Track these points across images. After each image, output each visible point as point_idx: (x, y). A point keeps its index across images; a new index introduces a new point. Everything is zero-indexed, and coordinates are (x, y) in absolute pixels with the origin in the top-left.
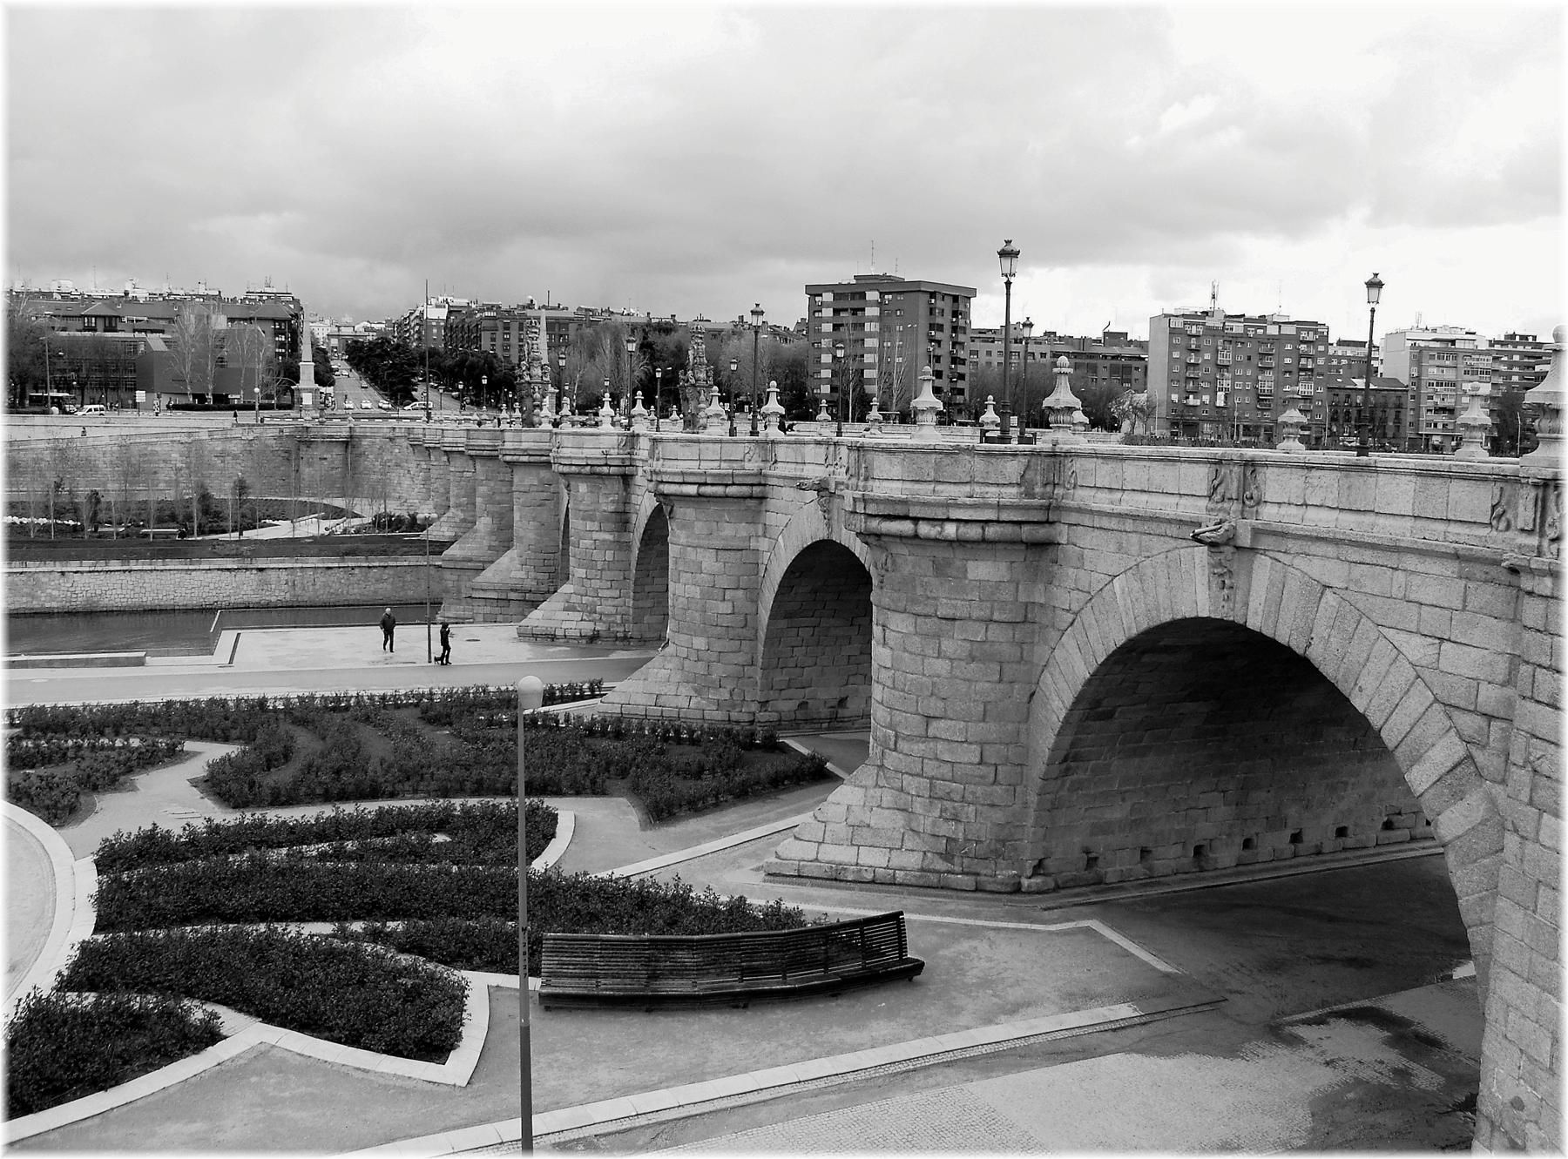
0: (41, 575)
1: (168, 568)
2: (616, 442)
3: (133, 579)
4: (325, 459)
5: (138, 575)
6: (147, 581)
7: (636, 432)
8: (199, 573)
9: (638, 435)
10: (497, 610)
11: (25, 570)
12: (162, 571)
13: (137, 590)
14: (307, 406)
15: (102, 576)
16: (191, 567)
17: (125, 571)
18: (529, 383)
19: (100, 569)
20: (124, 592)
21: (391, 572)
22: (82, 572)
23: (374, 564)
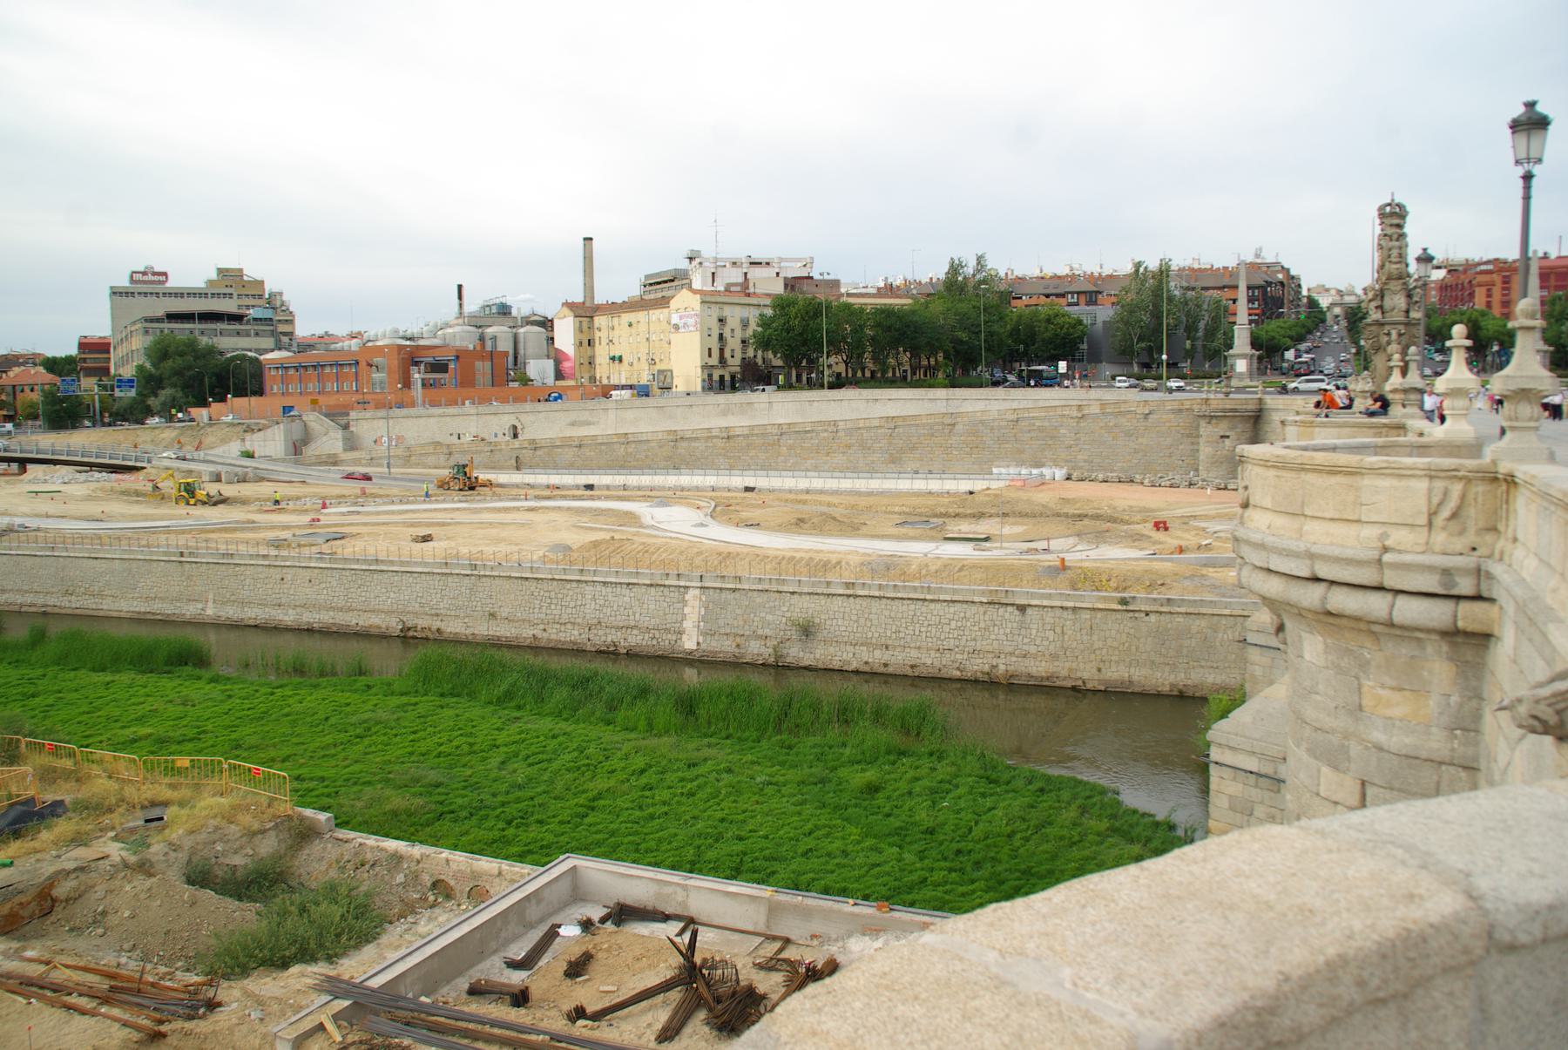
0: (755, 593)
1: (899, 595)
2: (1422, 505)
3: (858, 607)
4: (1228, 437)
5: (864, 603)
6: (874, 611)
7: (1504, 467)
8: (938, 606)
9: (1511, 481)
10: (1255, 793)
11: (738, 586)
12: (893, 599)
13: (862, 621)
14: (1241, 374)
15: (823, 600)
16: (928, 597)
17: (849, 596)
18: (1381, 324)
19: (819, 591)
20: (846, 623)
21: (1203, 623)
22: (801, 594)
23: (1179, 610)
